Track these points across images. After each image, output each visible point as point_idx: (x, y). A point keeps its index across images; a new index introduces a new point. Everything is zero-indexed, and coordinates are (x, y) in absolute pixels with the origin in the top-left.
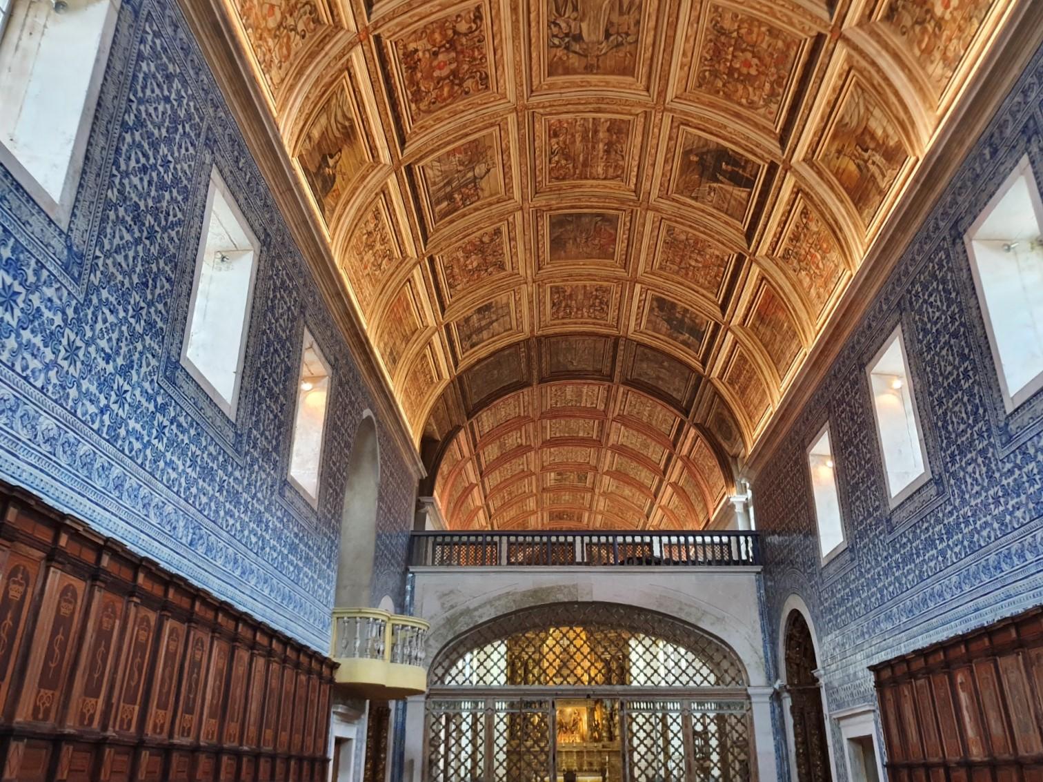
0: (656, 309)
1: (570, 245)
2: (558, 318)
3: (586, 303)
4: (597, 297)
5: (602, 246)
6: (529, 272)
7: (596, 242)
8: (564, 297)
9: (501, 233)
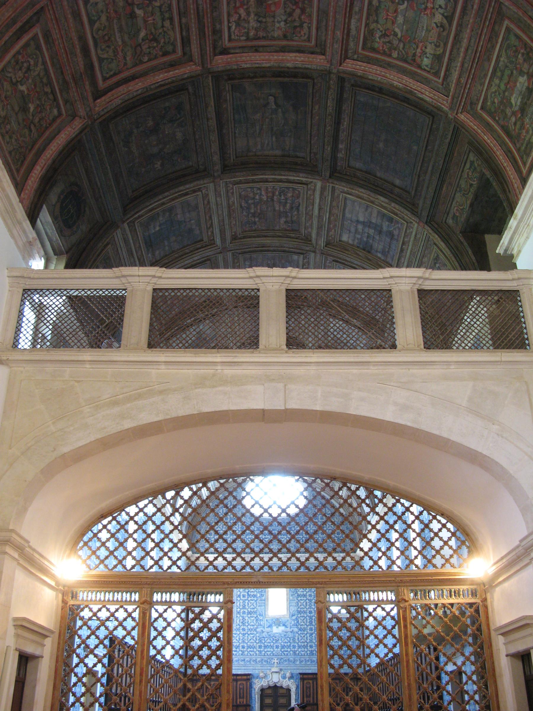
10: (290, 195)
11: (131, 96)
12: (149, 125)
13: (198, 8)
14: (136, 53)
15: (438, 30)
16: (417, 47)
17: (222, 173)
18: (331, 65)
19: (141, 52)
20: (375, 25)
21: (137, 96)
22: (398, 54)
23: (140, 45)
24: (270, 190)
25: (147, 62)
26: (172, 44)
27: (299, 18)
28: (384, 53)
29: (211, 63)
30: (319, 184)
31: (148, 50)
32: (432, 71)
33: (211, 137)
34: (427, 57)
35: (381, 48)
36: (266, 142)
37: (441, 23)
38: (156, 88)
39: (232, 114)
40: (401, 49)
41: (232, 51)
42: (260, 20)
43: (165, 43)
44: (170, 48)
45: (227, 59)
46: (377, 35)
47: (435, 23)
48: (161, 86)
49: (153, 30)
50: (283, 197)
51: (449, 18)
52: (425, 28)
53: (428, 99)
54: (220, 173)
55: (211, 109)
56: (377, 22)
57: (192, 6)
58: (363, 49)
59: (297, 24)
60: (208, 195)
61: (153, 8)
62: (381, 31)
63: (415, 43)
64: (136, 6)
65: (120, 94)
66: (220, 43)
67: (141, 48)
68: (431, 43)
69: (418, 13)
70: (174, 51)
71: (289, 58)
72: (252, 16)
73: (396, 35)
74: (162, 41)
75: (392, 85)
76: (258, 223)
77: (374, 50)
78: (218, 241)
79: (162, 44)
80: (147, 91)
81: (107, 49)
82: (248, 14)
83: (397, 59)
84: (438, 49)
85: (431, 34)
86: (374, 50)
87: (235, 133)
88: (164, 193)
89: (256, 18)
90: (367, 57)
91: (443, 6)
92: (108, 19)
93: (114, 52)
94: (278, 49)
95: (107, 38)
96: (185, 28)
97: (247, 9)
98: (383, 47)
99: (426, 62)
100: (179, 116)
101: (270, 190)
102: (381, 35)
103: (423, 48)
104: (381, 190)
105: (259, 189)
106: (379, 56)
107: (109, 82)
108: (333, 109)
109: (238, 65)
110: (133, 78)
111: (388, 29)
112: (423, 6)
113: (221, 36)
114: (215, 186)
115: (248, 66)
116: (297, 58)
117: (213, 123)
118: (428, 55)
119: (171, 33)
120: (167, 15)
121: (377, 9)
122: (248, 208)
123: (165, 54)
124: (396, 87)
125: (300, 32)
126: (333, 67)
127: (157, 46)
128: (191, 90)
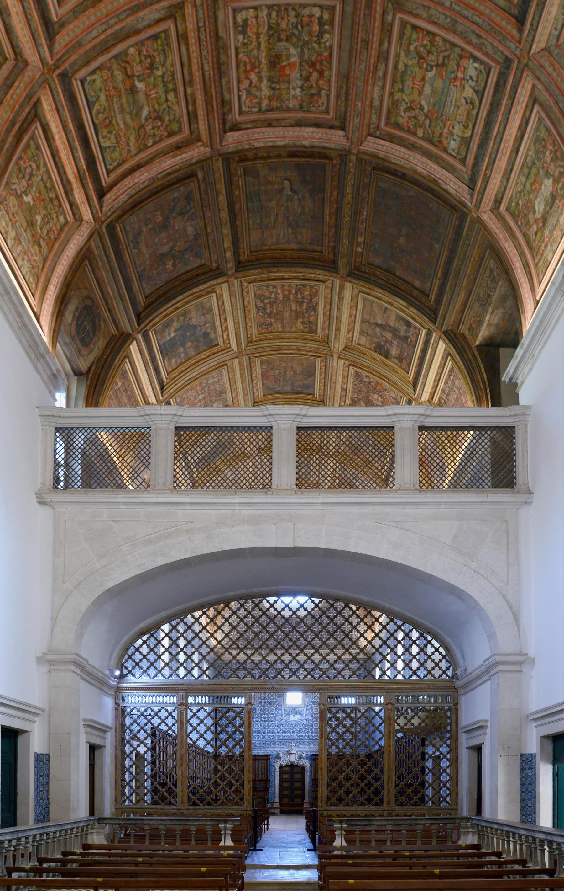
0: (209, 331)
1: (299, 369)
2: (312, 287)
3: (280, 307)
4: (270, 315)
5: (272, 369)
6: (335, 364)
7: (277, 372)
8: (304, 317)
9: (352, 399)
10: (307, 293)
11: (137, 189)
12: (158, 221)
13: (203, 75)
14: (140, 136)
15: (467, 107)
16: (444, 126)
17: (236, 271)
18: (351, 144)
19: (145, 134)
20: (400, 94)
21: (144, 189)
22: (424, 133)
23: (143, 126)
24: (286, 288)
25: (152, 145)
26: (178, 122)
27: (317, 83)
28: (409, 131)
29: (221, 143)
30: (338, 282)
31: (152, 131)
32: (459, 157)
33: (224, 231)
34: (454, 140)
35: (406, 124)
36: (282, 235)
37: (472, 99)
38: (164, 177)
39: (245, 203)
40: (427, 127)
41: (244, 126)
42: (273, 86)
43: (170, 121)
44: (175, 127)
45: (238, 137)
46: (402, 108)
47: (465, 98)
48: (169, 174)
49: (156, 106)
50: (299, 296)
51: (480, 94)
52: (453, 103)
53: (452, 191)
54: (234, 270)
55: (222, 198)
56: (402, 91)
57: (197, 74)
58: (387, 124)
59: (313, 91)
60: (222, 295)
61: (155, 79)
62: (407, 103)
63: (442, 121)
64: (136, 78)
65: (125, 188)
66: (230, 116)
67: (144, 129)
68: (459, 122)
69: (448, 84)
70: (180, 131)
71: (305, 134)
72: (265, 81)
73: (422, 109)
74: (167, 118)
75: (415, 171)
76: (274, 324)
77: (398, 126)
78: (234, 346)
79: (167, 122)
80: (154, 181)
81: (109, 135)
82: (260, 79)
83: (422, 138)
84: (466, 131)
85: (460, 111)
86: (398, 126)
87: (249, 224)
88: (177, 297)
89: (269, 84)
90: (389, 134)
91: (475, 79)
92: (109, 98)
93: (116, 137)
94: (293, 122)
95: (107, 121)
96: (190, 100)
97: (259, 72)
98: (408, 122)
99: (453, 145)
100: (188, 208)
101: (286, 288)
102: (406, 108)
103: (451, 128)
104: (400, 292)
105: (275, 287)
106: (403, 135)
107: (113, 176)
108: (352, 197)
109: (250, 144)
110: (139, 167)
111: (414, 101)
112: (453, 75)
113: (231, 108)
114: (229, 285)
115: (261, 144)
116: (315, 134)
117: (224, 214)
118: (455, 137)
119: (176, 108)
120: (170, 86)
121: (404, 73)
122: (264, 309)
123: (171, 134)
124: (420, 174)
125: (317, 101)
126: (353, 146)
127: (162, 125)
128: (200, 176)
